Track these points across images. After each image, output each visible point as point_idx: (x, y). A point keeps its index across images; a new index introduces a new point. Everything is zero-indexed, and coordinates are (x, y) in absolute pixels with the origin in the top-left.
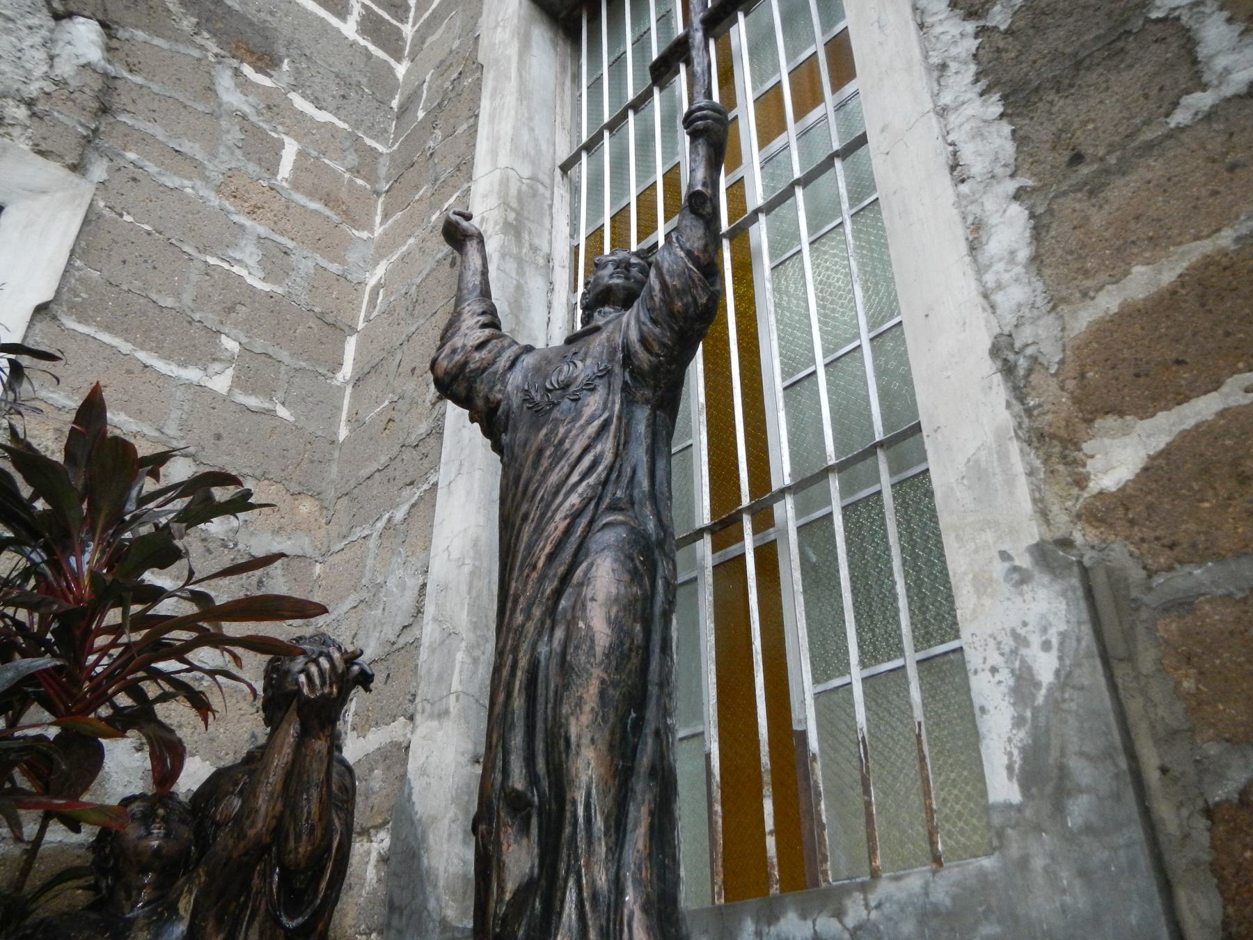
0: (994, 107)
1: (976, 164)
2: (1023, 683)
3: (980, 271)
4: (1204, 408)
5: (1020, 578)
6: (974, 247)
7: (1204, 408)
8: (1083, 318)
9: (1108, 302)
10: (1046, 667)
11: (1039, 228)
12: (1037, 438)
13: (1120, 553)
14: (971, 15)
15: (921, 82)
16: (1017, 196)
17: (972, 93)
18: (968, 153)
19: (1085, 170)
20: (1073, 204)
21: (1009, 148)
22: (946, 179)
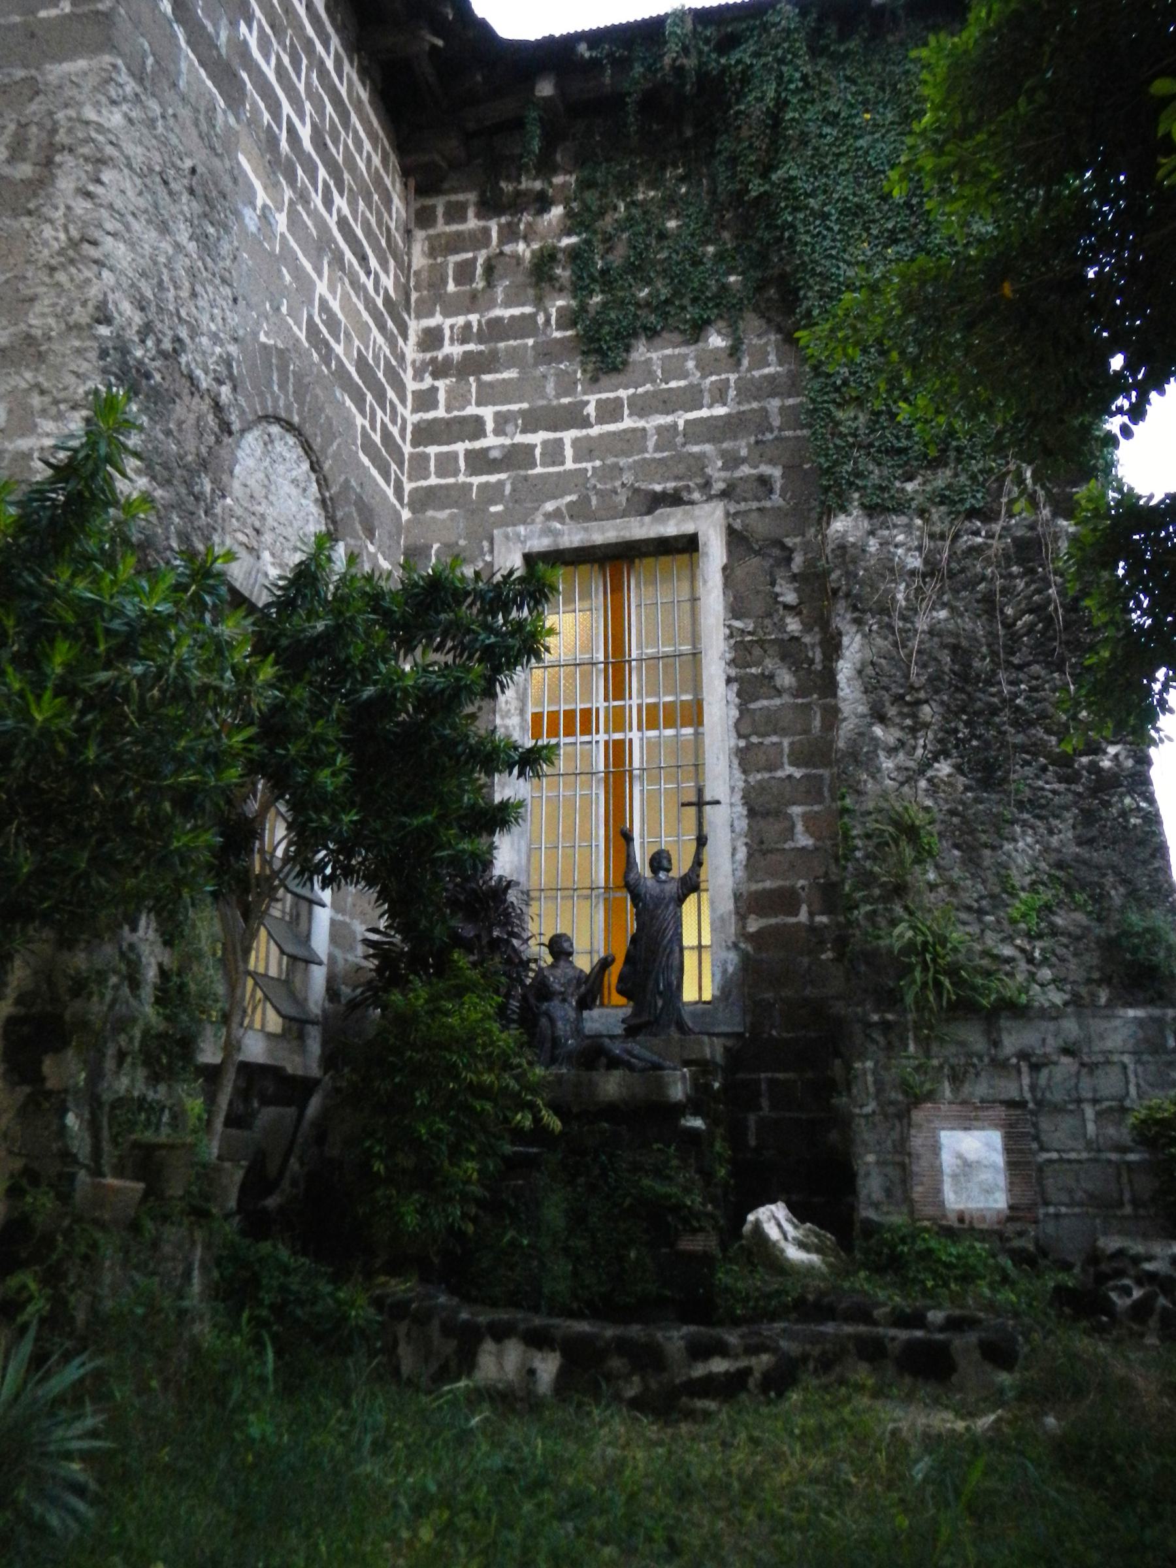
0: (745, 812)
1: (738, 830)
2: (725, 971)
3: (733, 862)
4: (773, 921)
5: (728, 948)
6: (733, 855)
7: (773, 921)
8: (755, 887)
9: (760, 886)
10: (731, 969)
11: (750, 856)
12: (737, 913)
13: (750, 949)
14: (745, 772)
15: (728, 791)
16: (746, 844)
17: (740, 803)
18: (736, 823)
19: (764, 847)
20: (757, 855)
21: (746, 827)
22: (728, 830)
